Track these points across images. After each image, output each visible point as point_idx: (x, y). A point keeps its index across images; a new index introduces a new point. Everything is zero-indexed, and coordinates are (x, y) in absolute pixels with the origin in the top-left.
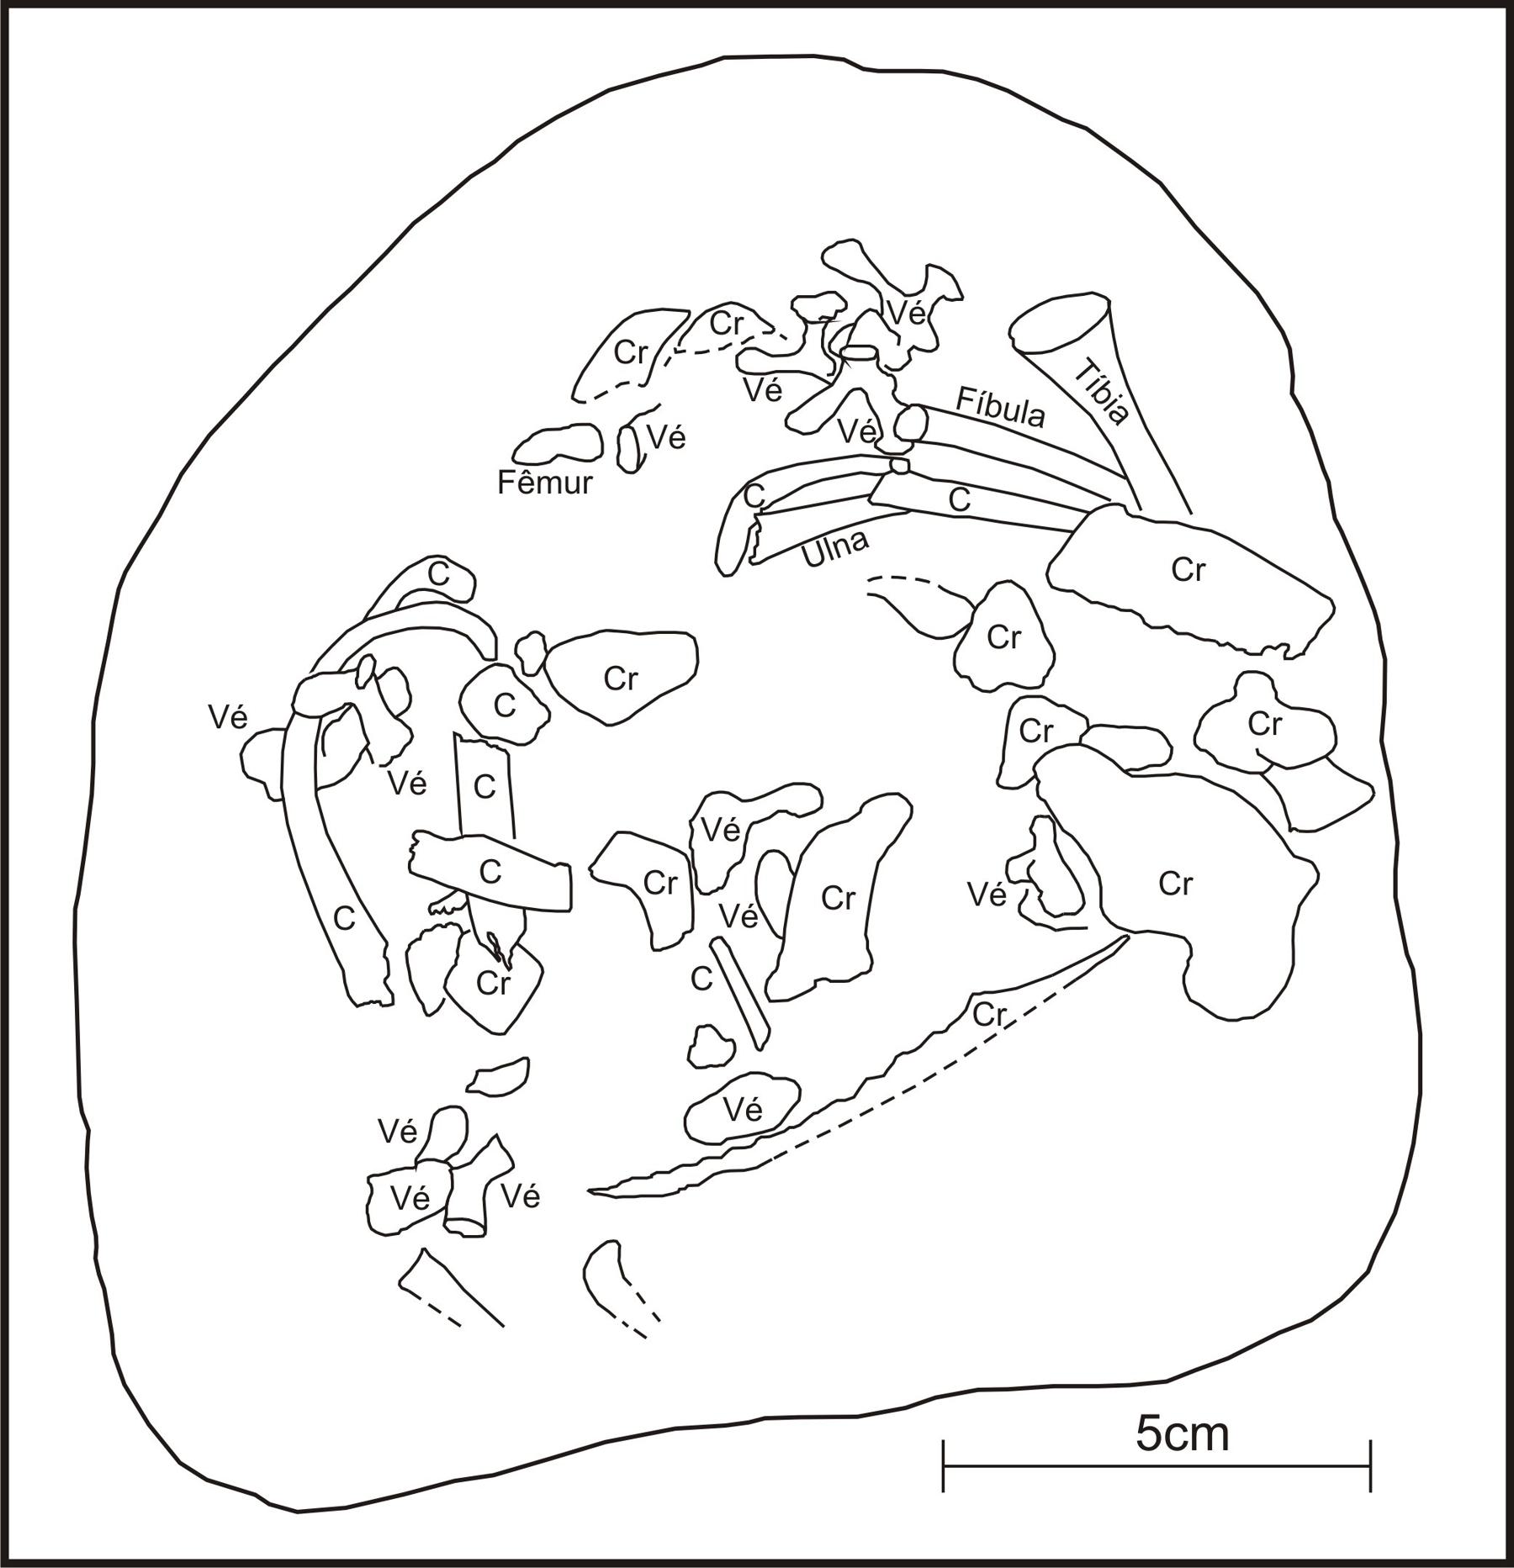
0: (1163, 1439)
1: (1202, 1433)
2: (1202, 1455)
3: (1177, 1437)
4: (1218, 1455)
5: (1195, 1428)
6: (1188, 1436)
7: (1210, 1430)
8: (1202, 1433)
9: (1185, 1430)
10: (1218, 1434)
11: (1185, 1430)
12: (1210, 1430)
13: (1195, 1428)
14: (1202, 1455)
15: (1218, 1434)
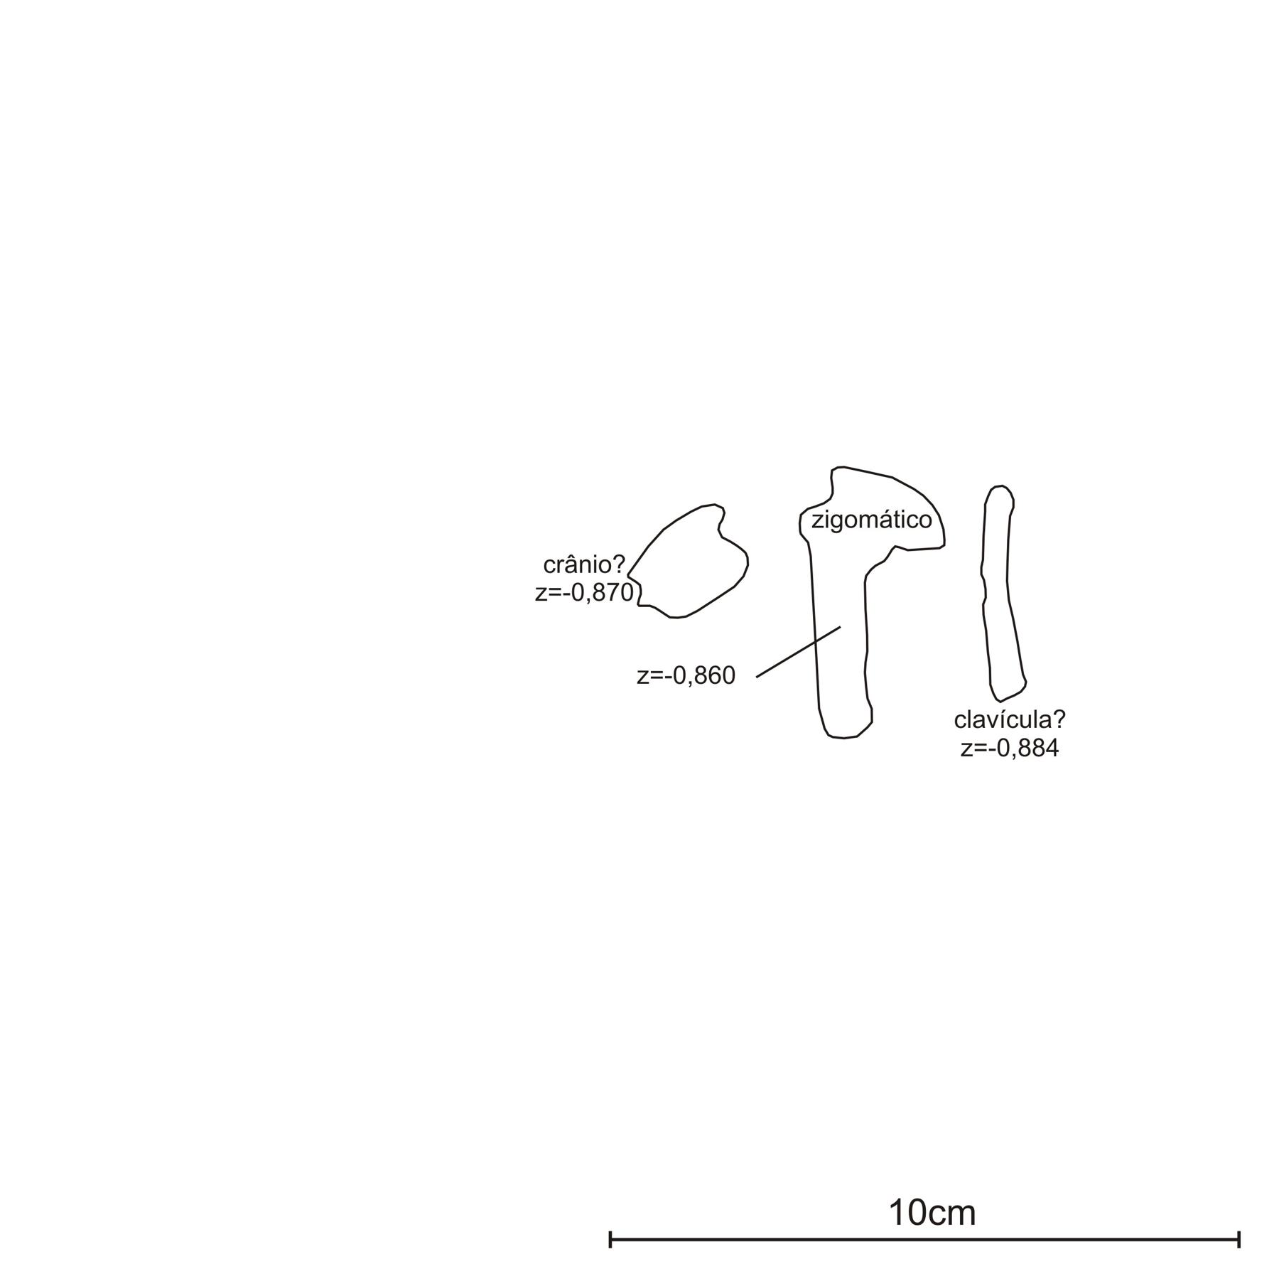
0: (928, 1214)
1: (956, 1212)
2: (955, 1230)
3: (938, 1216)
4: (967, 1230)
5: (951, 1209)
6: (946, 1215)
7: (962, 1210)
8: (956, 1212)
9: (943, 1210)
10: (967, 1213)
11: (943, 1210)
12: (962, 1210)
13: (951, 1209)
14: (955, 1230)
15: (967, 1213)
